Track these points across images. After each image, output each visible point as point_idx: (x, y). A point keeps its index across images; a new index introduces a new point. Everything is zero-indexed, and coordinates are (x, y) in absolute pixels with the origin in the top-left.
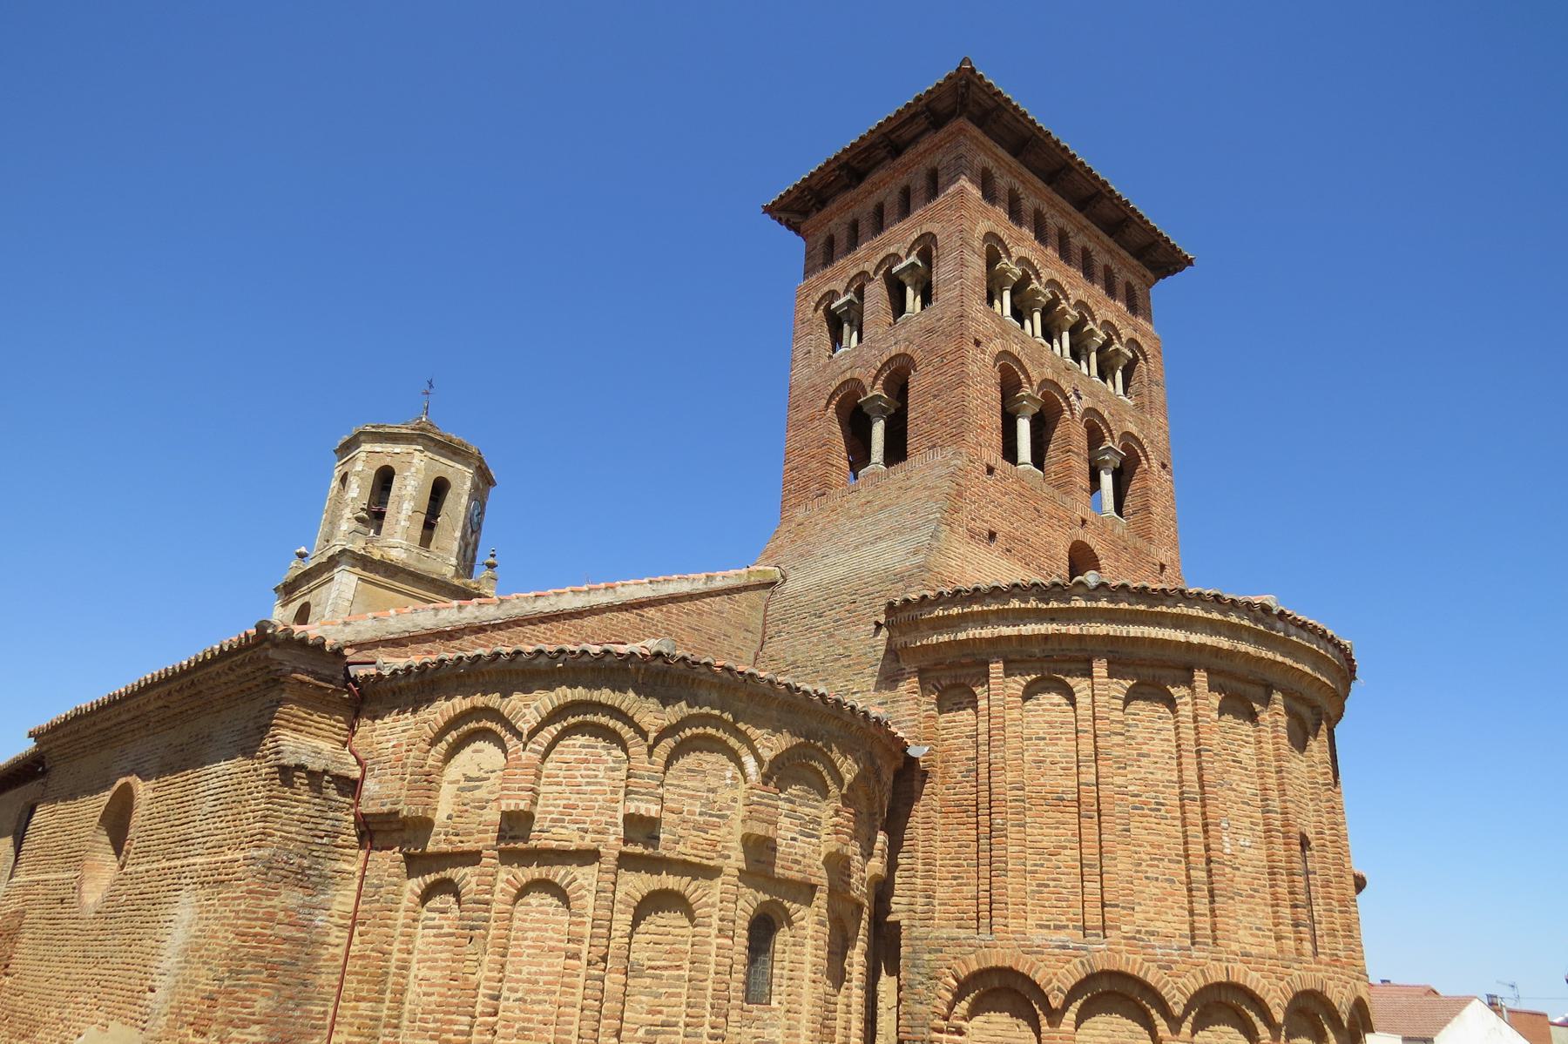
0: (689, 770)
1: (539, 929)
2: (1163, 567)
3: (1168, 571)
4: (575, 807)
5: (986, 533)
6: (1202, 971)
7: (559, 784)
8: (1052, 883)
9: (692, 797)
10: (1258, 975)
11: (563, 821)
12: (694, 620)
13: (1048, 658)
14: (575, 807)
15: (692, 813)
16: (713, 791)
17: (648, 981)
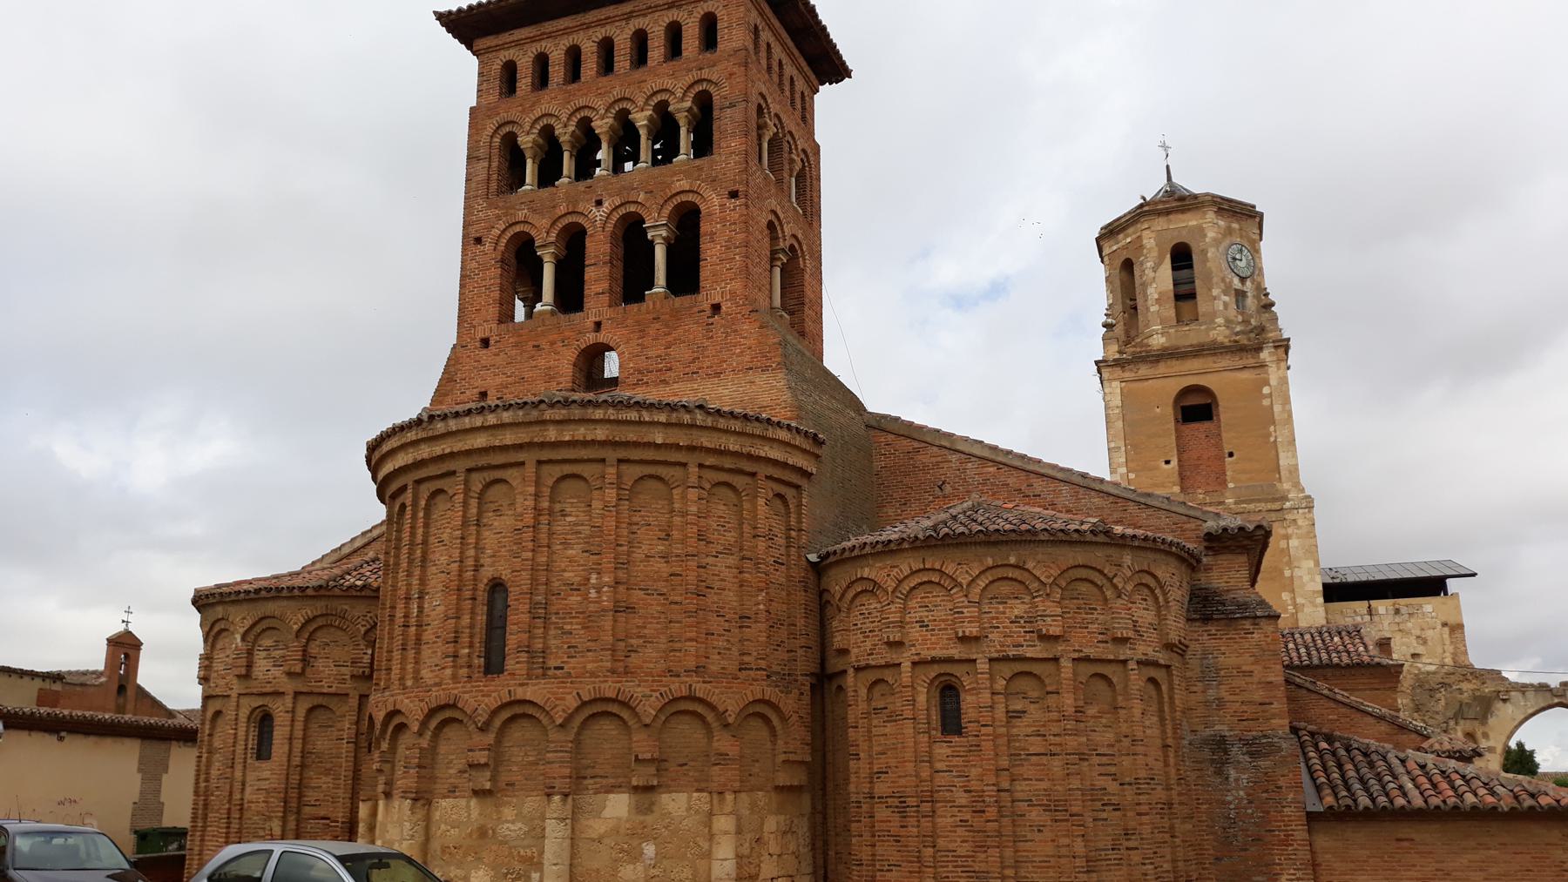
2: (716, 308)
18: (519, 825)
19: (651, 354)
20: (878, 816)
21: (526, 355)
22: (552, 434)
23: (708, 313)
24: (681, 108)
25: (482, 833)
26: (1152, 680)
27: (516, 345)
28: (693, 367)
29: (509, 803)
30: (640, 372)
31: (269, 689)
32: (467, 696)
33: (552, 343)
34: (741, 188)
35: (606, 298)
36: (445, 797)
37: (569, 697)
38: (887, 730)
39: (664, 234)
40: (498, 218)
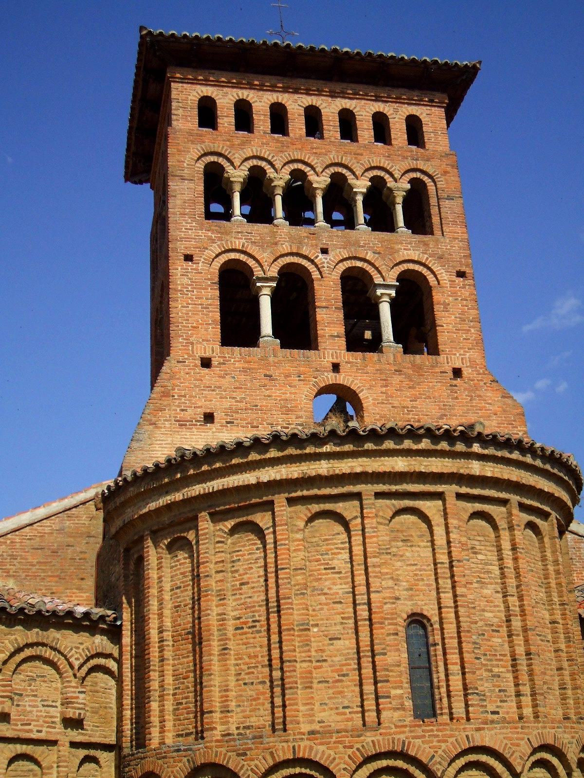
3: (466, 372)
6: (272, 754)
8: (184, 701)
10: (321, 748)
12: (36, 542)
13: (172, 525)
19: (396, 403)
21: (257, 383)
22: (476, 468)
23: (451, 374)
27: (244, 371)
32: (418, 742)
34: (468, 270)
35: (343, 342)
37: (522, 743)
39: (393, 293)
40: (213, 241)
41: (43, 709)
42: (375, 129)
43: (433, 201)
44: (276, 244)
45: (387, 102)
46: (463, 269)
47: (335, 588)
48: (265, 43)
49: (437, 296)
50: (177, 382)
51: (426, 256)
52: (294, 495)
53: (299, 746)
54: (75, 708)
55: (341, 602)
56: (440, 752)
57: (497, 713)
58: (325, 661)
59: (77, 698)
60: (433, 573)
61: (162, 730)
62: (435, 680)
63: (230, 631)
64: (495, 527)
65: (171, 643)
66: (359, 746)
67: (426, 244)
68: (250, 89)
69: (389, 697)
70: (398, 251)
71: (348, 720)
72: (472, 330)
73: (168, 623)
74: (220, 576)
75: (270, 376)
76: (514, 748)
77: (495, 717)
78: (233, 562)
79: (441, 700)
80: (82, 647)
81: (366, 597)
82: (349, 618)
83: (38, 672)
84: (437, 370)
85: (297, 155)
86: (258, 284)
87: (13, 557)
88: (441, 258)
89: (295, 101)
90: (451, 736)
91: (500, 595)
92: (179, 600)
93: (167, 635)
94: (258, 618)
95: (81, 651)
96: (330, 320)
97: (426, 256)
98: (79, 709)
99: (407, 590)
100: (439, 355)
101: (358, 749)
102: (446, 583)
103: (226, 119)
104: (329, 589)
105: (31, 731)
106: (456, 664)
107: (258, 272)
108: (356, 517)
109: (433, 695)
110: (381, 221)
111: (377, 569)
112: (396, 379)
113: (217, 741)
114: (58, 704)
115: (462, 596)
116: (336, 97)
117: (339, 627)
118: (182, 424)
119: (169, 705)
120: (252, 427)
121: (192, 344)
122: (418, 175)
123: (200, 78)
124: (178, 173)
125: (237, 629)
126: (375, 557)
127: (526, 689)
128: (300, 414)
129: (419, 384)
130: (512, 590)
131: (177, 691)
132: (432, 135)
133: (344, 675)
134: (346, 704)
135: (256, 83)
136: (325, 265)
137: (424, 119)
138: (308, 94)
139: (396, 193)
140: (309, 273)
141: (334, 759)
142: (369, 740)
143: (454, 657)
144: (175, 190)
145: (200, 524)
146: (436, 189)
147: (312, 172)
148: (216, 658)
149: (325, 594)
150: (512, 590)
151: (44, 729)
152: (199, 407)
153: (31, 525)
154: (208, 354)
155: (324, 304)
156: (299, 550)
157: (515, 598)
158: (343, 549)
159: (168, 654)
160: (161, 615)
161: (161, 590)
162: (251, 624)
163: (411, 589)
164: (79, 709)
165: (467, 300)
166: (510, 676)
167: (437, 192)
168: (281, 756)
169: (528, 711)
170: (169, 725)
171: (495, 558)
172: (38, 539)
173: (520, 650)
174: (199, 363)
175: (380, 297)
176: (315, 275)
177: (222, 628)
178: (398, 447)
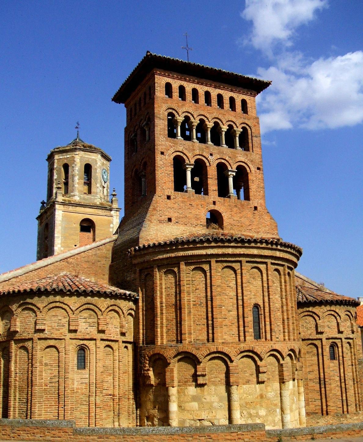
0: (53, 316)
1: (24, 357)
2: (256, 208)
3: (259, 208)
4: (27, 328)
5: (167, 220)
6: (209, 349)
7: (23, 323)
8: (171, 329)
9: (55, 322)
10: (226, 348)
11: (24, 332)
12: (86, 259)
13: (168, 264)
14: (27, 328)
15: (55, 326)
16: (60, 320)
17: (49, 367)
18: (273, 393)
19: (235, 219)
20: (309, 385)
22: (278, 254)
23: (253, 209)
24: (239, 130)
25: (262, 396)
26: (349, 343)
27: (182, 202)
28: (250, 228)
29: (269, 385)
30: (231, 225)
31: (88, 337)
32: (257, 347)
33: (197, 205)
34: (261, 167)
35: (217, 193)
36: (244, 384)
38: (313, 359)
39: (234, 174)
41: (114, 329)
42: (230, 104)
43: (250, 137)
44: (194, 150)
45: (235, 92)
46: (260, 166)
47: (231, 293)
48: (194, 64)
49: (250, 177)
50: (158, 205)
51: (247, 160)
52: (218, 259)
53: (219, 347)
54: (125, 329)
55: (232, 299)
56: (263, 351)
57: (278, 338)
58: (226, 318)
59: (125, 325)
60: (261, 290)
61: (162, 338)
62: (261, 327)
63: (192, 306)
64: (280, 274)
65: (165, 308)
66: (239, 348)
67: (247, 155)
68: (185, 81)
69: (248, 332)
70: (237, 157)
71: (233, 339)
72: (262, 192)
73: (164, 300)
74: (188, 286)
75: (191, 205)
76: (284, 350)
77: (277, 339)
78: (193, 281)
79: (262, 333)
80: (126, 306)
81: (241, 297)
82: (235, 304)
83: (113, 315)
84: (249, 207)
85: (202, 113)
86: (187, 166)
87: (78, 265)
88: (252, 161)
89: (201, 88)
90: (267, 346)
91: (280, 298)
92: (169, 292)
93: (164, 305)
94: (202, 302)
95: (126, 308)
96: (213, 184)
97: (247, 160)
98: (126, 329)
99: (254, 295)
100: (250, 200)
101: (238, 349)
102: (266, 294)
103: (175, 93)
104: (229, 293)
105: (111, 337)
106: (268, 321)
107: (187, 161)
108: (239, 269)
109: (260, 331)
110: (231, 144)
111: (246, 288)
112: (235, 209)
113: (187, 344)
114: (119, 327)
115: (272, 299)
116: (216, 88)
117: (232, 307)
118: (160, 222)
119: (165, 330)
120: (185, 225)
121: (164, 189)
122: (245, 125)
123: (167, 74)
124: (158, 116)
125: (194, 305)
126: (246, 284)
127: (286, 331)
128: (202, 221)
129: (242, 211)
130: (284, 297)
131: (168, 325)
132: (250, 109)
133: (233, 324)
134: (233, 333)
135: (188, 79)
136: (211, 161)
137: (248, 101)
138: (206, 86)
139: (237, 132)
140: (205, 163)
141: (231, 352)
142: (242, 346)
143: (267, 319)
144: (157, 123)
145: (181, 266)
146: (251, 132)
147: (207, 120)
148: (186, 315)
149: (227, 295)
150: (284, 297)
151: (115, 336)
152: (166, 215)
153: (84, 252)
154: (169, 194)
155: (211, 177)
156: (219, 279)
157: (285, 299)
158: (233, 280)
159: (164, 312)
160: (161, 298)
161: (161, 288)
162: (199, 304)
163: (255, 295)
164: (126, 329)
165: (260, 179)
166: (282, 326)
167: (251, 133)
168: (212, 350)
169: (287, 338)
170: (165, 337)
171: (279, 285)
172: (87, 258)
173: (285, 317)
174: (166, 197)
175: (230, 175)
176: (208, 164)
177: (189, 305)
178: (255, 246)
